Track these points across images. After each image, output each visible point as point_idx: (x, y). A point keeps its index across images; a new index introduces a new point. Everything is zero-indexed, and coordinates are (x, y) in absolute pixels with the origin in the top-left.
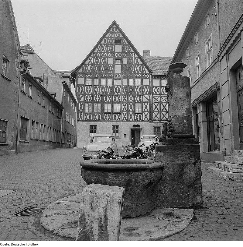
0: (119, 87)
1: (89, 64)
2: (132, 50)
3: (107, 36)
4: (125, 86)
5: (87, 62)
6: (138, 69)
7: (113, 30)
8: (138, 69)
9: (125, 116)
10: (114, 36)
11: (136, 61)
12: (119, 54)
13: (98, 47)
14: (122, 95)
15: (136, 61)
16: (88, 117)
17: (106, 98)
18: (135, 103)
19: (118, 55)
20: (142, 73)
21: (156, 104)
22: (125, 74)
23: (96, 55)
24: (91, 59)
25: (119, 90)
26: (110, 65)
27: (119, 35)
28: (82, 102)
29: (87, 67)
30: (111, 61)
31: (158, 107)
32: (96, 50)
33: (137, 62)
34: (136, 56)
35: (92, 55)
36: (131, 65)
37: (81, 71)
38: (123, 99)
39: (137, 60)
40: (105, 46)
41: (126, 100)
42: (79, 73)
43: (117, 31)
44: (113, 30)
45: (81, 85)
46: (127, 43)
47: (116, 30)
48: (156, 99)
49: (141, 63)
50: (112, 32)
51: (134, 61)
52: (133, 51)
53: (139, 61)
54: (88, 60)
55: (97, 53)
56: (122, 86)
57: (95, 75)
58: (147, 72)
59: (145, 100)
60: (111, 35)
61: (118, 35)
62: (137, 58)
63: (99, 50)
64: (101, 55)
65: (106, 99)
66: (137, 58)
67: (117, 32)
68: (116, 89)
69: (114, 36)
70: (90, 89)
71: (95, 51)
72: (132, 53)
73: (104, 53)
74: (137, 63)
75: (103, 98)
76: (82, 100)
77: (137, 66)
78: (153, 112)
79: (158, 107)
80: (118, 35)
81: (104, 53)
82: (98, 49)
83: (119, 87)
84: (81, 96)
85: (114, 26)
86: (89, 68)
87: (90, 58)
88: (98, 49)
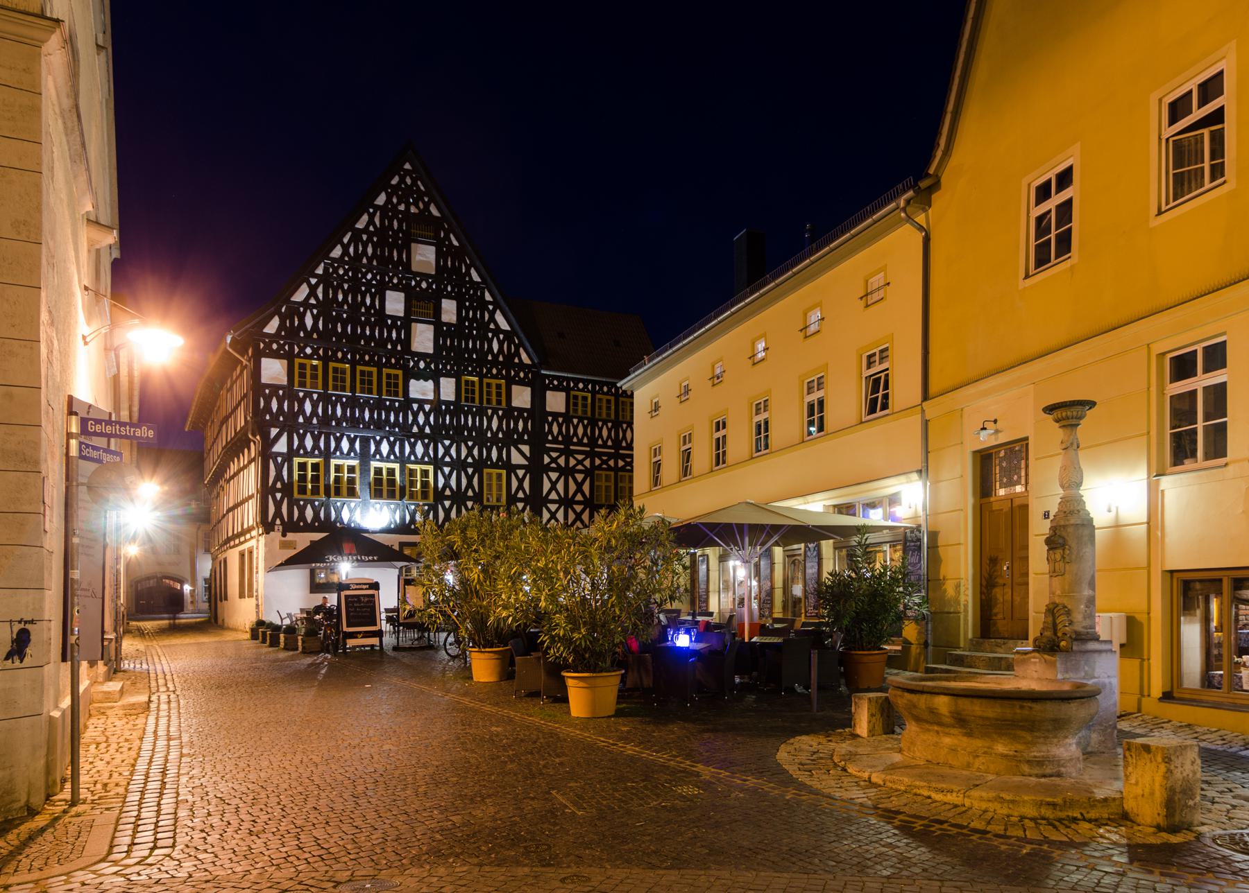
0: (427, 407)
4: (447, 403)
6: (495, 346)
7: (402, 180)
8: (495, 346)
10: (408, 208)
14: (435, 438)
18: (480, 465)
21: (554, 476)
25: (427, 415)
26: (394, 318)
27: (427, 205)
28: (279, 454)
29: (302, 317)
30: (395, 304)
31: (560, 486)
33: (492, 319)
36: (471, 328)
39: (492, 314)
40: (370, 240)
43: (418, 187)
44: (402, 180)
46: (455, 243)
51: (482, 316)
56: (437, 403)
57: (335, 353)
59: (517, 459)
60: (395, 200)
61: (421, 205)
64: (355, 274)
66: (491, 307)
67: (421, 195)
68: (415, 415)
69: (408, 208)
70: (315, 406)
74: (492, 326)
77: (490, 335)
78: (546, 501)
83: (427, 407)
86: (309, 321)
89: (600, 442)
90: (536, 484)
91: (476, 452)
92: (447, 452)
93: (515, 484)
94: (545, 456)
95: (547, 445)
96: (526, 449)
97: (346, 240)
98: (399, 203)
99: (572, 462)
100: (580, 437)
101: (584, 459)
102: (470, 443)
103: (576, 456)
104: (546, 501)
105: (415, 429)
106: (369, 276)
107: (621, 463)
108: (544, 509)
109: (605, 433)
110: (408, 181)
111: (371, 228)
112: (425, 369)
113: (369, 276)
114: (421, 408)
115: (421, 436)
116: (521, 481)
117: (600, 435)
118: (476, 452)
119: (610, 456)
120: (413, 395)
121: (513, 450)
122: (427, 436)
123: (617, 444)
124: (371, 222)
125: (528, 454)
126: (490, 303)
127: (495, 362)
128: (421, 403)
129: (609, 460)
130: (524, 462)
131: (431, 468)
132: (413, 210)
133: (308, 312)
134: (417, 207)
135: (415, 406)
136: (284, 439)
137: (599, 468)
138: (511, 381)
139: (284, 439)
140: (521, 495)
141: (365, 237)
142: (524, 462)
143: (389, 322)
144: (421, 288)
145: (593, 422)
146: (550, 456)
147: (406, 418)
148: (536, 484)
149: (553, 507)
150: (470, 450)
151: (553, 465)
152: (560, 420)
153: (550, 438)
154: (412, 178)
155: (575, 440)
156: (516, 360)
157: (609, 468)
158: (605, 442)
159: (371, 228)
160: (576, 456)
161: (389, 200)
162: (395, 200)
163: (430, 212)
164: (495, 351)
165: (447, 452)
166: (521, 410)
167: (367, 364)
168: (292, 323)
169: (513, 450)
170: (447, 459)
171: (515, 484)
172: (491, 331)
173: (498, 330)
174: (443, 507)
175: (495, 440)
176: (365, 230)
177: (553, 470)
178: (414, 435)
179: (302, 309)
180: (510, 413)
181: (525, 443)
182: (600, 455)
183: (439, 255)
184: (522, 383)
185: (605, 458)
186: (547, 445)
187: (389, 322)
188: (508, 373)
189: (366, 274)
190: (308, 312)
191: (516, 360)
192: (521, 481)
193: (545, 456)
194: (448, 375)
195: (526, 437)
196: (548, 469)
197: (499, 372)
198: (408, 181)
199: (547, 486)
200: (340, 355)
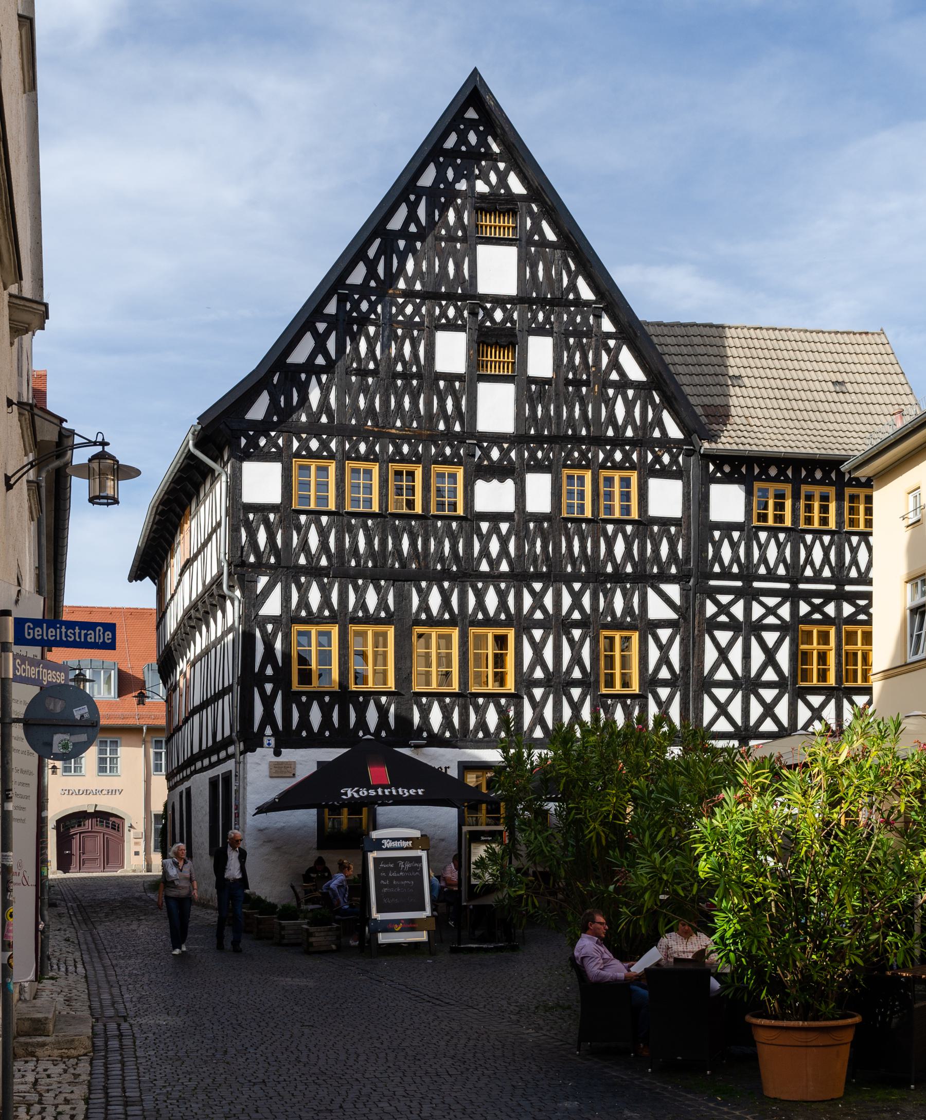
0: (504, 527)
1: (310, 367)
2: (581, 284)
3: (428, 178)
4: (539, 518)
5: (299, 356)
7: (463, 139)
8: (620, 411)
9: (538, 707)
11: (605, 359)
12: (504, 310)
13: (371, 252)
15: (605, 359)
16: (316, 716)
17: (424, 596)
19: (498, 315)
20: (642, 442)
21: (724, 637)
22: (539, 440)
23: (356, 305)
24: (327, 333)
25: (504, 542)
26: (450, 378)
27: (503, 178)
31: (736, 656)
32: (358, 276)
33: (615, 364)
34: (607, 325)
35: (331, 308)
36: (577, 383)
37: (258, 411)
38: (528, 601)
39: (614, 356)
41: (544, 610)
42: (254, 424)
43: (489, 147)
44: (463, 139)
45: (261, 509)
46: (551, 236)
47: (482, 141)
48: (724, 609)
49: (635, 372)
50: (455, 152)
52: (587, 294)
53: (626, 358)
54: (307, 344)
55: (363, 290)
58: (674, 432)
59: (657, 609)
60: (450, 174)
61: (493, 178)
62: (612, 343)
63: (372, 273)
65: (424, 606)
66: (612, 343)
69: (472, 187)
71: (350, 281)
72: (579, 302)
73: (409, 294)
74: (614, 376)
75: (403, 599)
76: (272, 607)
77: (611, 392)
78: (707, 684)
79: (736, 656)
80: (493, 178)
81: (409, 294)
82: (372, 267)
84: (263, 581)
85: (471, 114)
87: (321, 327)
88: (372, 267)
89: (808, 572)
90: (692, 652)
91: (586, 601)
92: (538, 603)
93: (654, 654)
94: (708, 602)
95: (712, 583)
96: (673, 591)
97: (371, 252)
98: (457, 179)
99: (757, 611)
100: (772, 565)
101: (779, 605)
102: (577, 586)
103: (763, 599)
104: (707, 684)
105: (484, 567)
106: (409, 310)
107: (848, 609)
108: (706, 698)
109: (818, 555)
110: (472, 138)
111: (413, 228)
112: (500, 460)
113: (409, 310)
114: (495, 530)
115: (493, 577)
116: (664, 649)
117: (809, 561)
118: (586, 601)
119: (828, 597)
120: (480, 506)
121: (651, 594)
122: (503, 576)
123: (839, 577)
124: (412, 217)
125: (677, 600)
126: (609, 335)
127: (619, 441)
128: (495, 518)
129: (825, 604)
130: (671, 615)
131: (511, 634)
132: (481, 187)
133: (314, 379)
134: (488, 182)
135: (485, 526)
136: (276, 594)
137: (807, 619)
138: (649, 471)
139: (276, 594)
140: (664, 674)
141: (402, 244)
142: (671, 615)
143: (442, 384)
144: (493, 320)
145: (796, 535)
146: (716, 603)
147: (469, 546)
148: (692, 652)
149: (722, 694)
150: (577, 597)
151: (723, 618)
152: (736, 535)
153: (717, 569)
154: (478, 133)
155: (762, 570)
156: (657, 434)
157: (827, 620)
158: (818, 573)
159: (413, 228)
160: (763, 599)
161: (441, 176)
162: (450, 174)
163: (507, 188)
164: (620, 421)
165: (538, 603)
166: (665, 522)
167: (404, 460)
168: (289, 399)
169: (651, 594)
170: (538, 615)
171: (654, 654)
172: (613, 384)
173: (624, 383)
174: (532, 698)
175: (618, 577)
176: (403, 232)
177: (723, 627)
178: (484, 577)
179: (303, 376)
180: (645, 523)
181: (671, 579)
182: (808, 596)
183: (525, 261)
184: (665, 473)
185: (817, 601)
186: (712, 583)
187: (442, 384)
188: (643, 457)
189: (404, 305)
190: (314, 379)
191: (657, 434)
192: (664, 649)
193: (708, 602)
194: (539, 468)
195: (673, 570)
196: (712, 625)
197: (627, 456)
198: (472, 138)
199: (711, 655)
200: (363, 448)
